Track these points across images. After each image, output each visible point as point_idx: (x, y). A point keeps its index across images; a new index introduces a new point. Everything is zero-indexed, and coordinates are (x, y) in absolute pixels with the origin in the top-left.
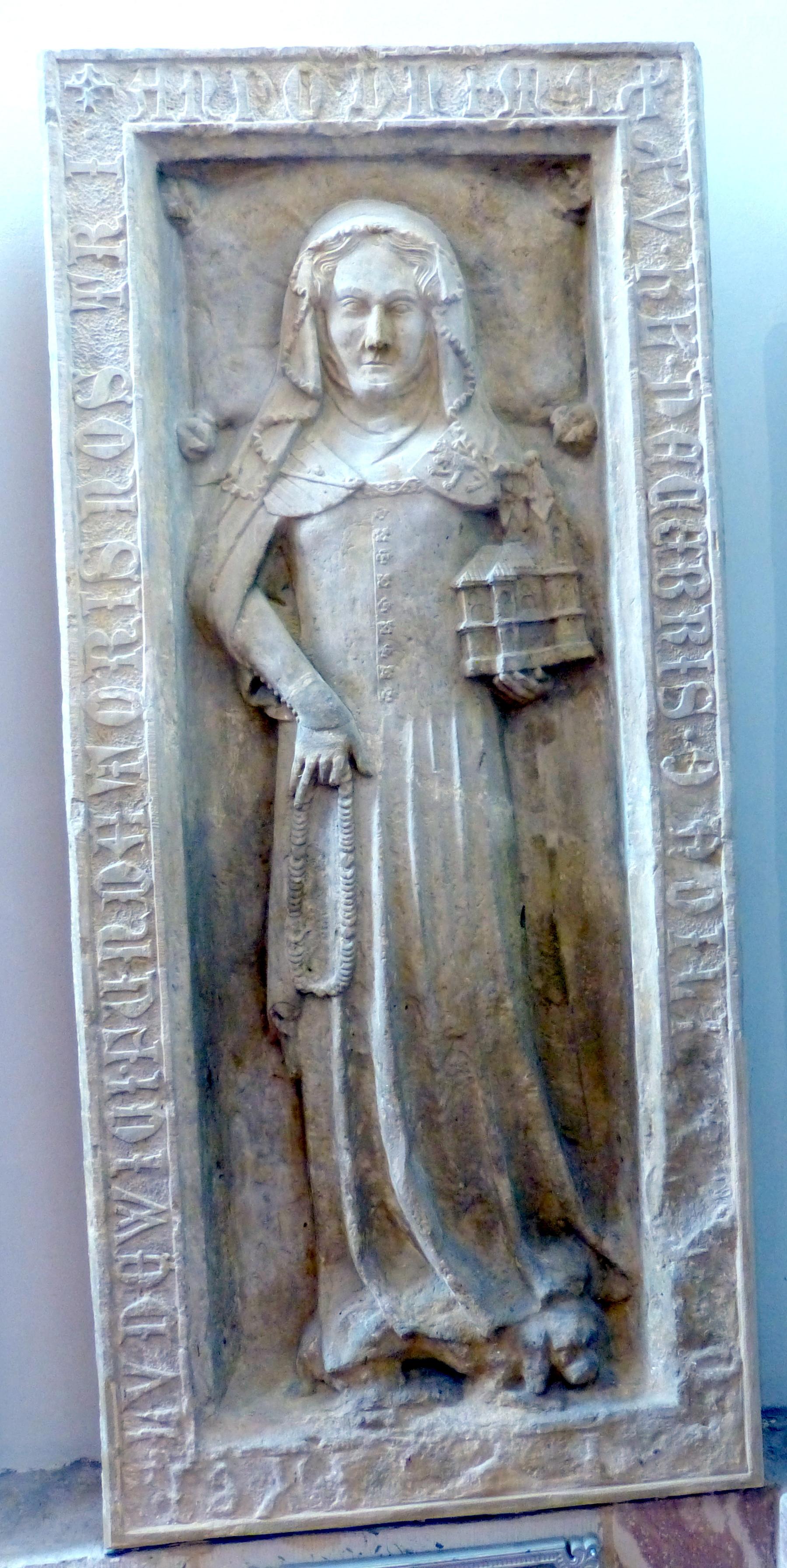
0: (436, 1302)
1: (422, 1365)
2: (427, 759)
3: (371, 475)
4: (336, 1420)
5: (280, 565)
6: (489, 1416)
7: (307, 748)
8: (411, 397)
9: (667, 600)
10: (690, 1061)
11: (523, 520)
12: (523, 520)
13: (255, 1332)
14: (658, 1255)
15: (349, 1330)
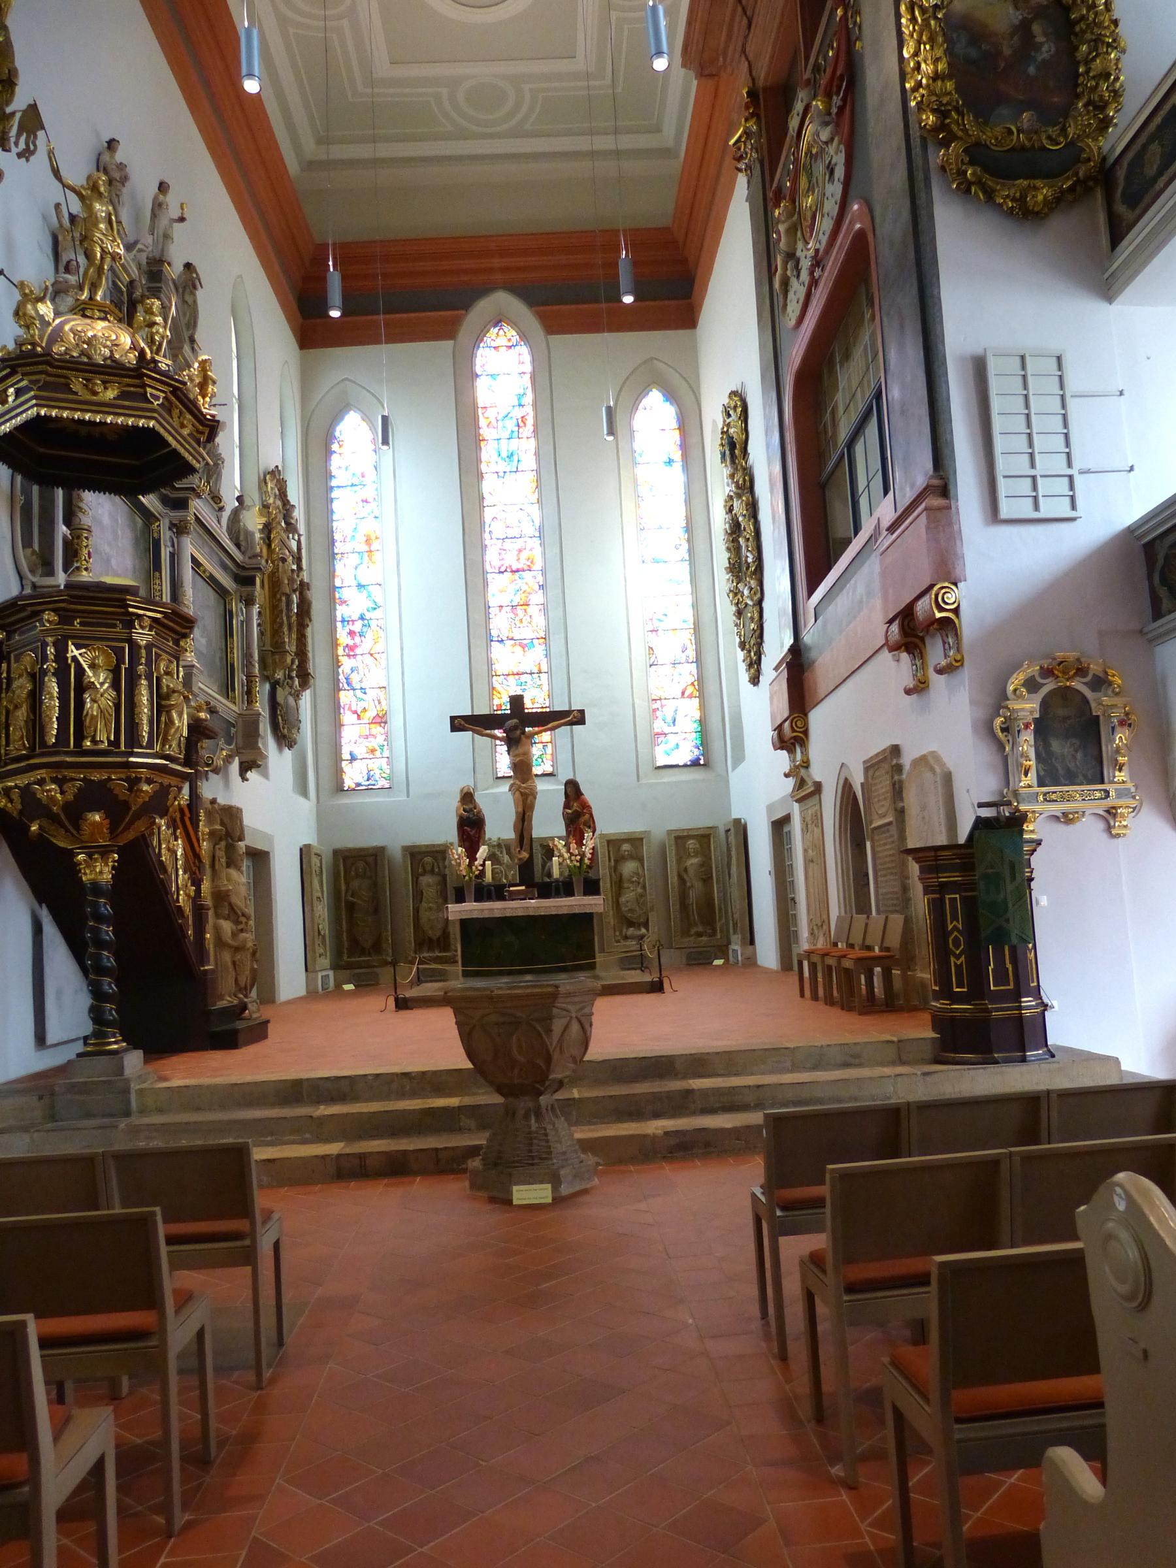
0: (700, 929)
1: (699, 935)
2: (698, 885)
3: (694, 861)
4: (692, 939)
5: (686, 870)
6: (704, 938)
7: (688, 884)
8: (696, 856)
9: (717, 872)
10: (720, 909)
11: (706, 865)
12: (706, 865)
13: (686, 933)
14: (718, 925)
15: (693, 931)
